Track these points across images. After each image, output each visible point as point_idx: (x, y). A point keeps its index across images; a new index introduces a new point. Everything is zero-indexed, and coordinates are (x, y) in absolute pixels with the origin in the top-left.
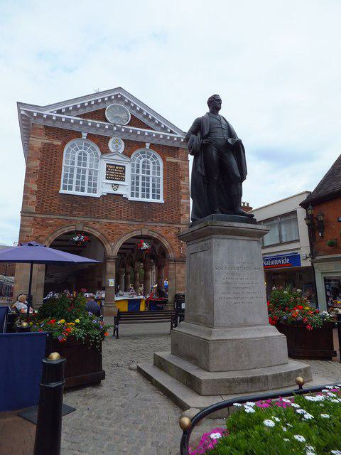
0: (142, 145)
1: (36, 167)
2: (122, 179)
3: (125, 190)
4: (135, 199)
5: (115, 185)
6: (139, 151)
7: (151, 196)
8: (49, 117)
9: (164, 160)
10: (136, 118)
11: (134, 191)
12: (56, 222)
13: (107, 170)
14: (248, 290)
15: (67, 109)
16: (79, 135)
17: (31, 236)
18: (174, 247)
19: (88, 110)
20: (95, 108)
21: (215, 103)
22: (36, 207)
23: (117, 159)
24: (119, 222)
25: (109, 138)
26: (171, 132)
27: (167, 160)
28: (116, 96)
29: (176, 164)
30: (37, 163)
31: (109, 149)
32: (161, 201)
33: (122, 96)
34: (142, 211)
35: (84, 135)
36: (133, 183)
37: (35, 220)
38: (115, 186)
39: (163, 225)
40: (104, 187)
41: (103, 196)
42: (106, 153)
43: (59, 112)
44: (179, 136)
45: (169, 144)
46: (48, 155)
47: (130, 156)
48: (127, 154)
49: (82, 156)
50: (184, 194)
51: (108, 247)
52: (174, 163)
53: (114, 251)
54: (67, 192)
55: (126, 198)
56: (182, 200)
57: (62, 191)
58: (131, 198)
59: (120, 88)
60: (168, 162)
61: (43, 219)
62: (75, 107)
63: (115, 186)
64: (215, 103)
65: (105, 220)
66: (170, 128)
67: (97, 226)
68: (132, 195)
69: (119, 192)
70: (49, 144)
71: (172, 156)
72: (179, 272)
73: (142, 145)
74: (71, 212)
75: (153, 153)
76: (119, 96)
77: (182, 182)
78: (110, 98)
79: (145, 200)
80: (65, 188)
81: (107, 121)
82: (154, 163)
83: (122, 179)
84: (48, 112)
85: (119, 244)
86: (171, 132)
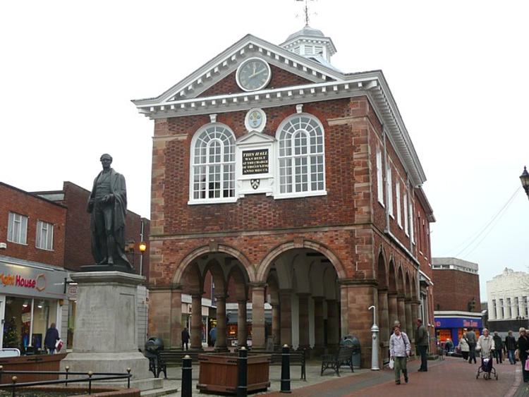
0: (291, 110)
1: (162, 175)
2: (265, 170)
3: (272, 186)
4: (287, 195)
5: (255, 180)
6: (289, 120)
7: (309, 187)
8: (168, 107)
9: (326, 126)
10: (280, 70)
11: (286, 185)
12: (186, 243)
13: (244, 161)
14: (98, 325)
15: (186, 90)
16: (206, 119)
17: (162, 265)
18: (345, 263)
19: (208, 85)
20: (217, 80)
21: (106, 160)
22: (165, 228)
23: (255, 142)
24: (262, 233)
25: (245, 112)
26: (328, 79)
27: (331, 123)
28: (247, 48)
29: (345, 128)
30: (163, 170)
31: (246, 130)
32: (324, 192)
33: (254, 45)
34: (292, 214)
35: (213, 117)
36: (282, 172)
37: (164, 244)
38: (255, 183)
39: (327, 229)
40: (243, 188)
41: (241, 199)
42: (243, 135)
43: (178, 97)
44: (340, 81)
45: (332, 96)
46: (173, 157)
47: (273, 135)
48: (270, 131)
49: (215, 147)
50: (359, 173)
51: (250, 271)
52: (342, 126)
53: (258, 275)
54: (200, 201)
55: (271, 197)
56: (356, 185)
57: (192, 201)
58: (278, 195)
59: (248, 35)
60: (332, 127)
61: (173, 242)
62: (195, 84)
63: (255, 183)
64: (106, 160)
65: (244, 234)
66: (325, 74)
67: (235, 243)
68: (282, 191)
69: (258, 191)
70: (173, 142)
71: (339, 114)
72: (354, 301)
73: (291, 110)
74: (203, 228)
75: (311, 117)
76: (250, 47)
77: (355, 155)
78: (238, 54)
79: (302, 194)
80: (196, 196)
81: (242, 91)
82: (312, 134)
83: (265, 170)
84: (164, 103)
85: (265, 264)
86: (328, 79)
